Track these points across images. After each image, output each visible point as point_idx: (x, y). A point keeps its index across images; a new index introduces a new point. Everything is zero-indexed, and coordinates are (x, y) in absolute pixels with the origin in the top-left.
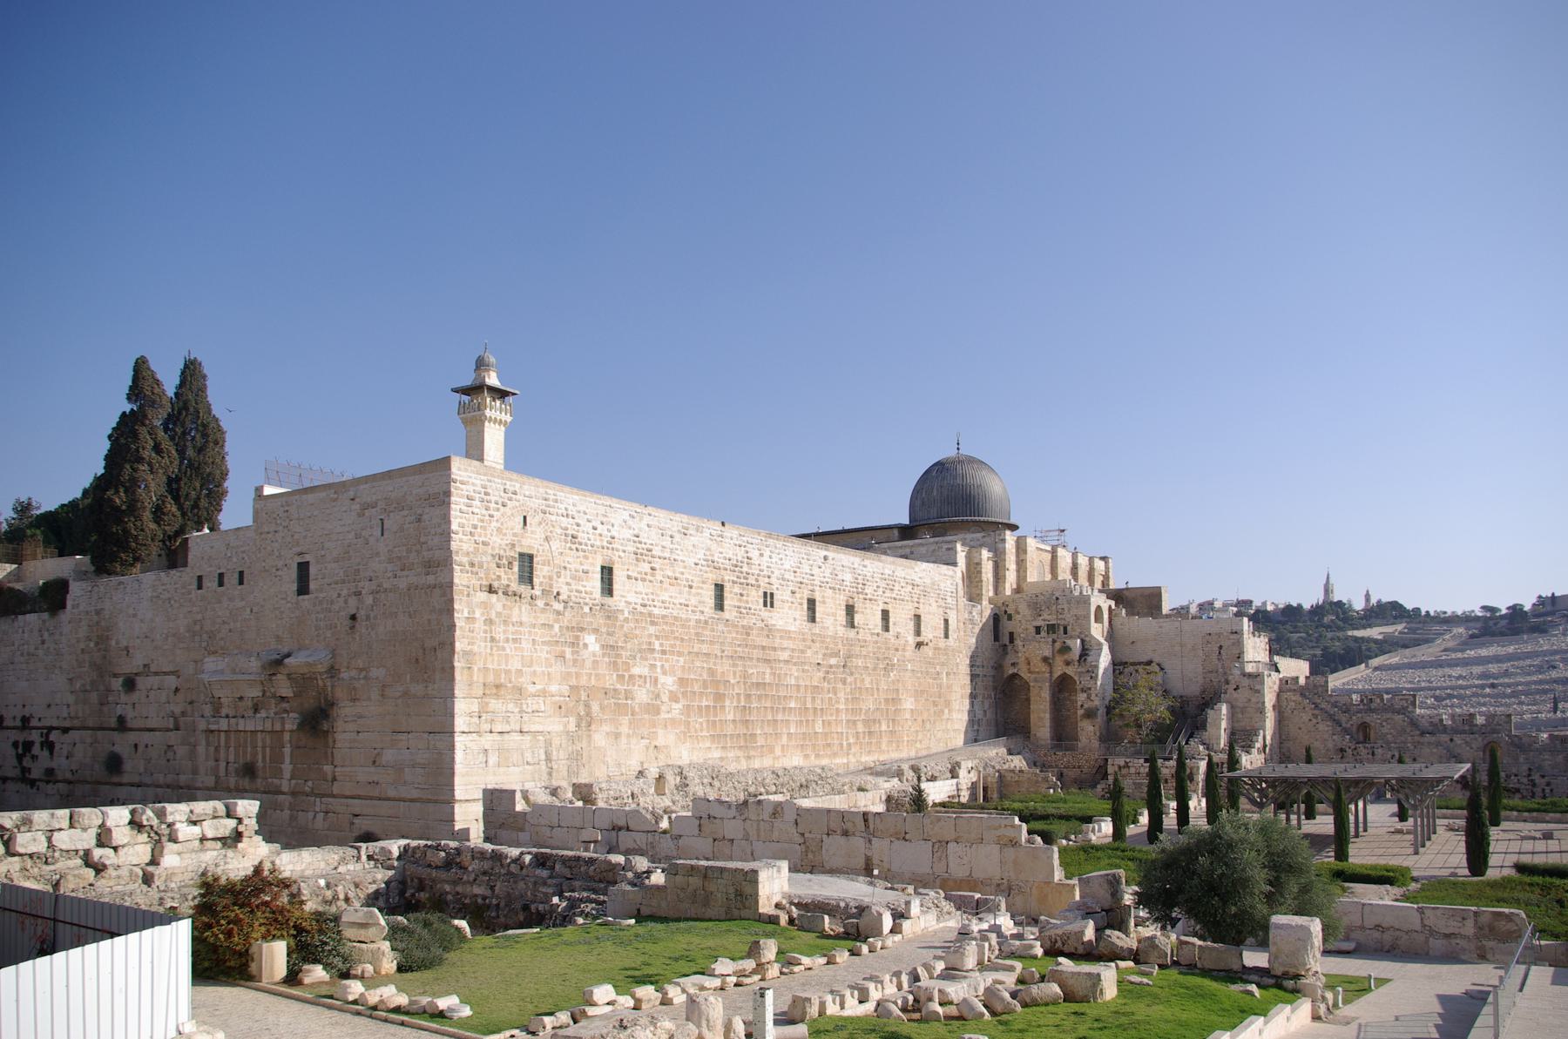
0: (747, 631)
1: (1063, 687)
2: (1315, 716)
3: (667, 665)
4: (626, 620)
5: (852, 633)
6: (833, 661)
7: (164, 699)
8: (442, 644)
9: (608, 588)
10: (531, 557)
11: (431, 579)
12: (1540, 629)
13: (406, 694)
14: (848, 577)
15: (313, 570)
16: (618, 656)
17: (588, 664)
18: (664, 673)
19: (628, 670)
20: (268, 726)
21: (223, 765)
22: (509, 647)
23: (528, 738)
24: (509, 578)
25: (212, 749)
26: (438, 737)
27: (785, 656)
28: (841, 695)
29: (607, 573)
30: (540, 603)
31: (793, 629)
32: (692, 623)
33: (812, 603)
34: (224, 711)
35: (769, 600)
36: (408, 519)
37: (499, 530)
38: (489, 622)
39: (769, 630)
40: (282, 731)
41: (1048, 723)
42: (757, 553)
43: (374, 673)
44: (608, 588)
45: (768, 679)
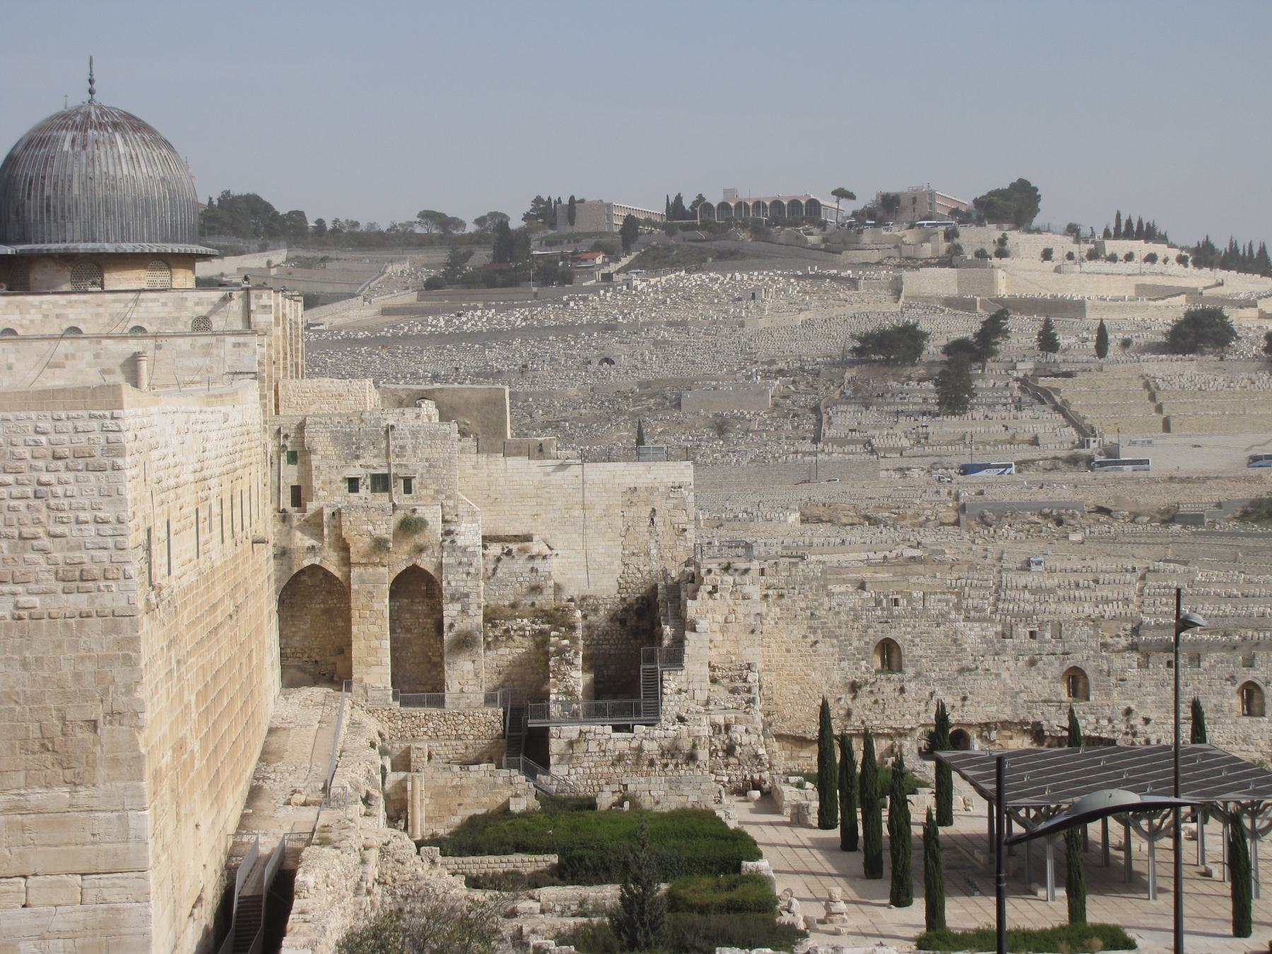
1: (417, 590)
2: (813, 630)
8: (114, 715)
11: (78, 602)
12: (555, 276)
26: (106, 880)
36: (16, 491)
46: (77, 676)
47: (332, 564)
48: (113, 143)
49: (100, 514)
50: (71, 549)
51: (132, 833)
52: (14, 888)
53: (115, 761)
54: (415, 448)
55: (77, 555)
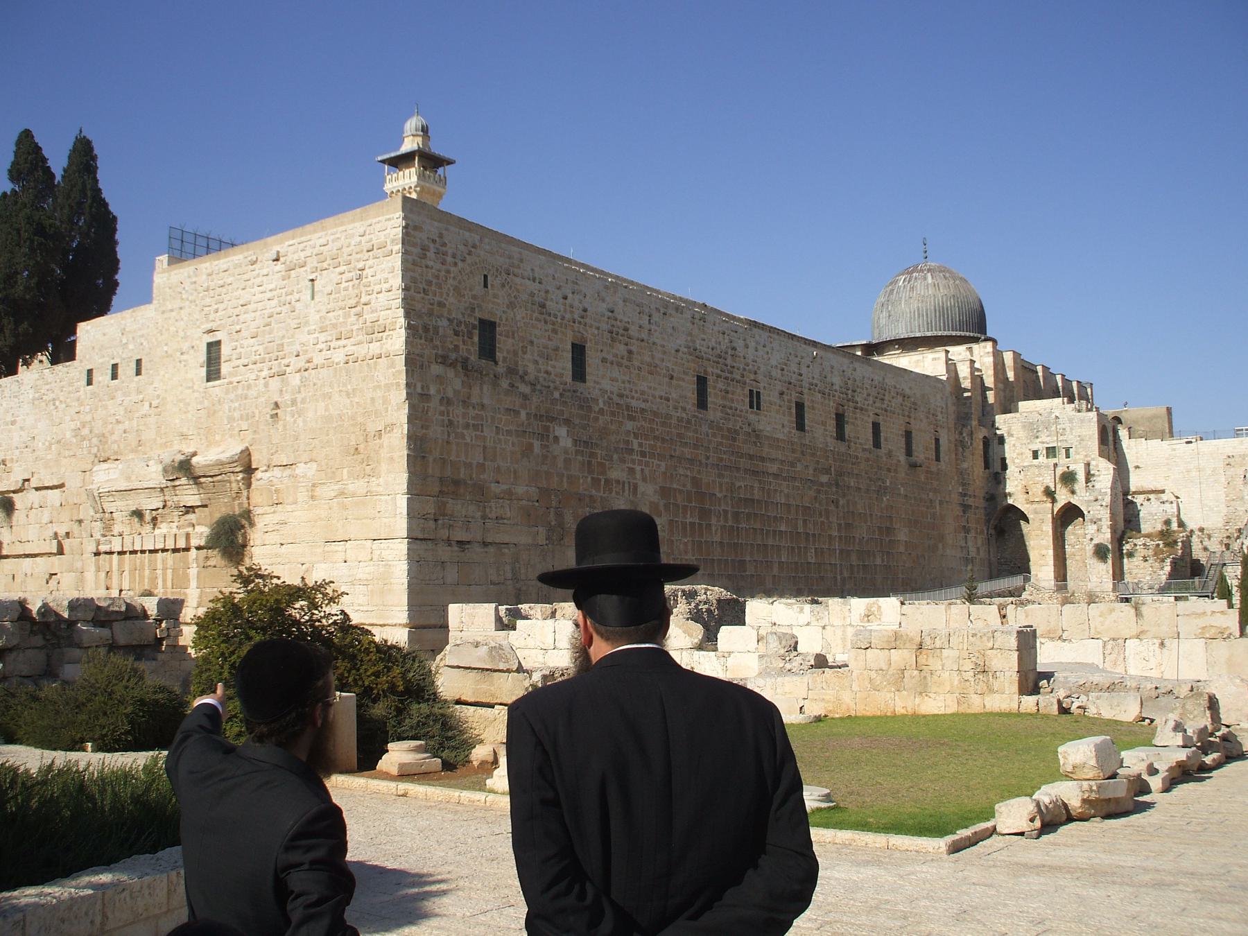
0: (733, 434)
3: (647, 471)
4: (601, 411)
5: (842, 447)
6: (824, 479)
7: (46, 519)
9: (579, 372)
10: (492, 325)
11: (375, 348)
13: (342, 493)
14: (837, 380)
15: (225, 350)
16: (592, 455)
17: (560, 464)
18: (644, 480)
19: (604, 473)
20: (170, 545)
22: (469, 435)
23: (491, 549)
24: (470, 348)
25: (103, 575)
26: (385, 544)
27: (773, 468)
28: (834, 519)
29: (579, 351)
30: (505, 384)
31: (781, 436)
32: (674, 421)
33: (800, 407)
34: (117, 529)
35: (755, 400)
36: (347, 276)
37: (456, 289)
38: (446, 401)
39: (756, 435)
40: (187, 549)
41: (1052, 562)
42: (741, 343)
43: (300, 469)
44: (579, 372)
45: (757, 495)
46: (373, 399)
48: (925, 279)
49: (386, 286)
50: (372, 312)
51: (398, 511)
52: (340, 549)
53: (392, 459)
54: (1071, 429)
55: (373, 316)
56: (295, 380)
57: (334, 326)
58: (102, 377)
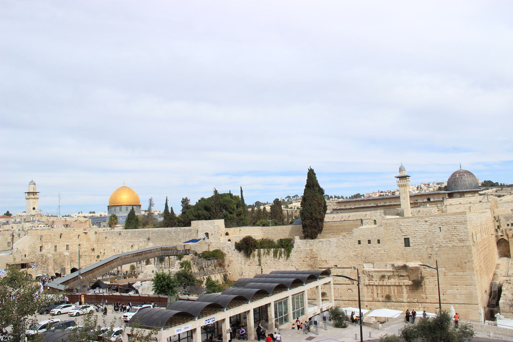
11: (462, 244)
15: (411, 241)
21: (375, 295)
26: (470, 287)
34: (374, 279)
47: (505, 238)
48: (464, 175)
55: (461, 237)
56: (437, 249)
57: (448, 238)
58: (365, 243)
